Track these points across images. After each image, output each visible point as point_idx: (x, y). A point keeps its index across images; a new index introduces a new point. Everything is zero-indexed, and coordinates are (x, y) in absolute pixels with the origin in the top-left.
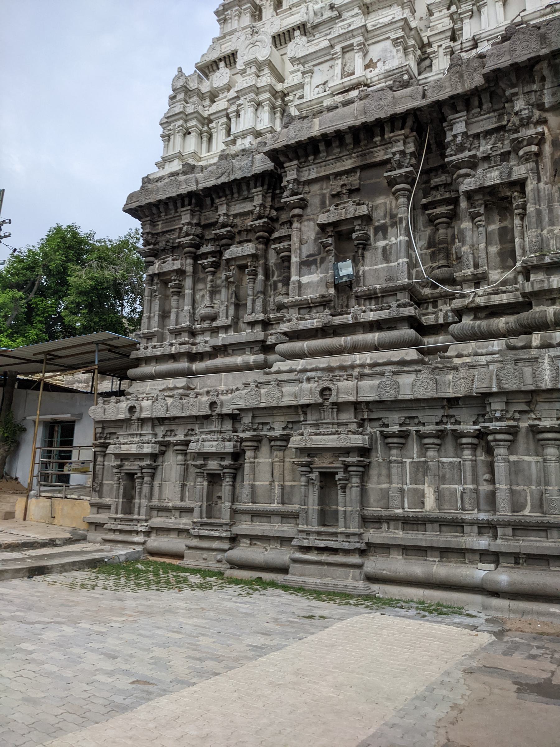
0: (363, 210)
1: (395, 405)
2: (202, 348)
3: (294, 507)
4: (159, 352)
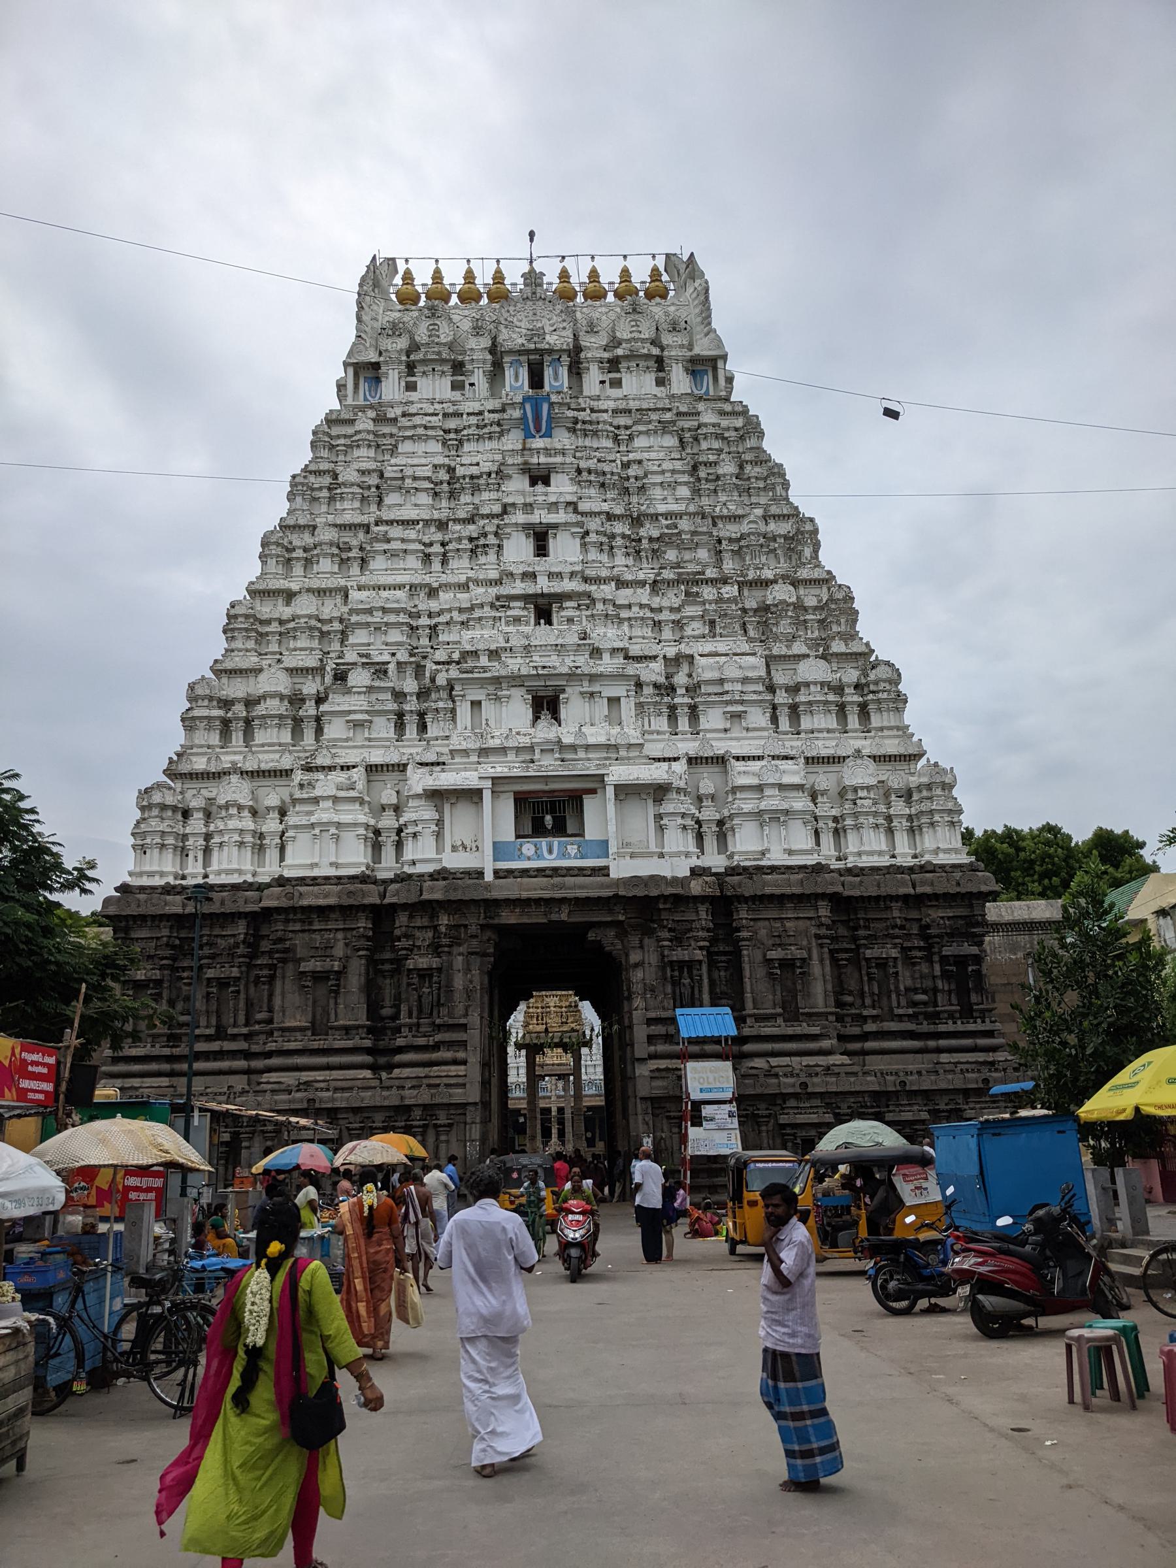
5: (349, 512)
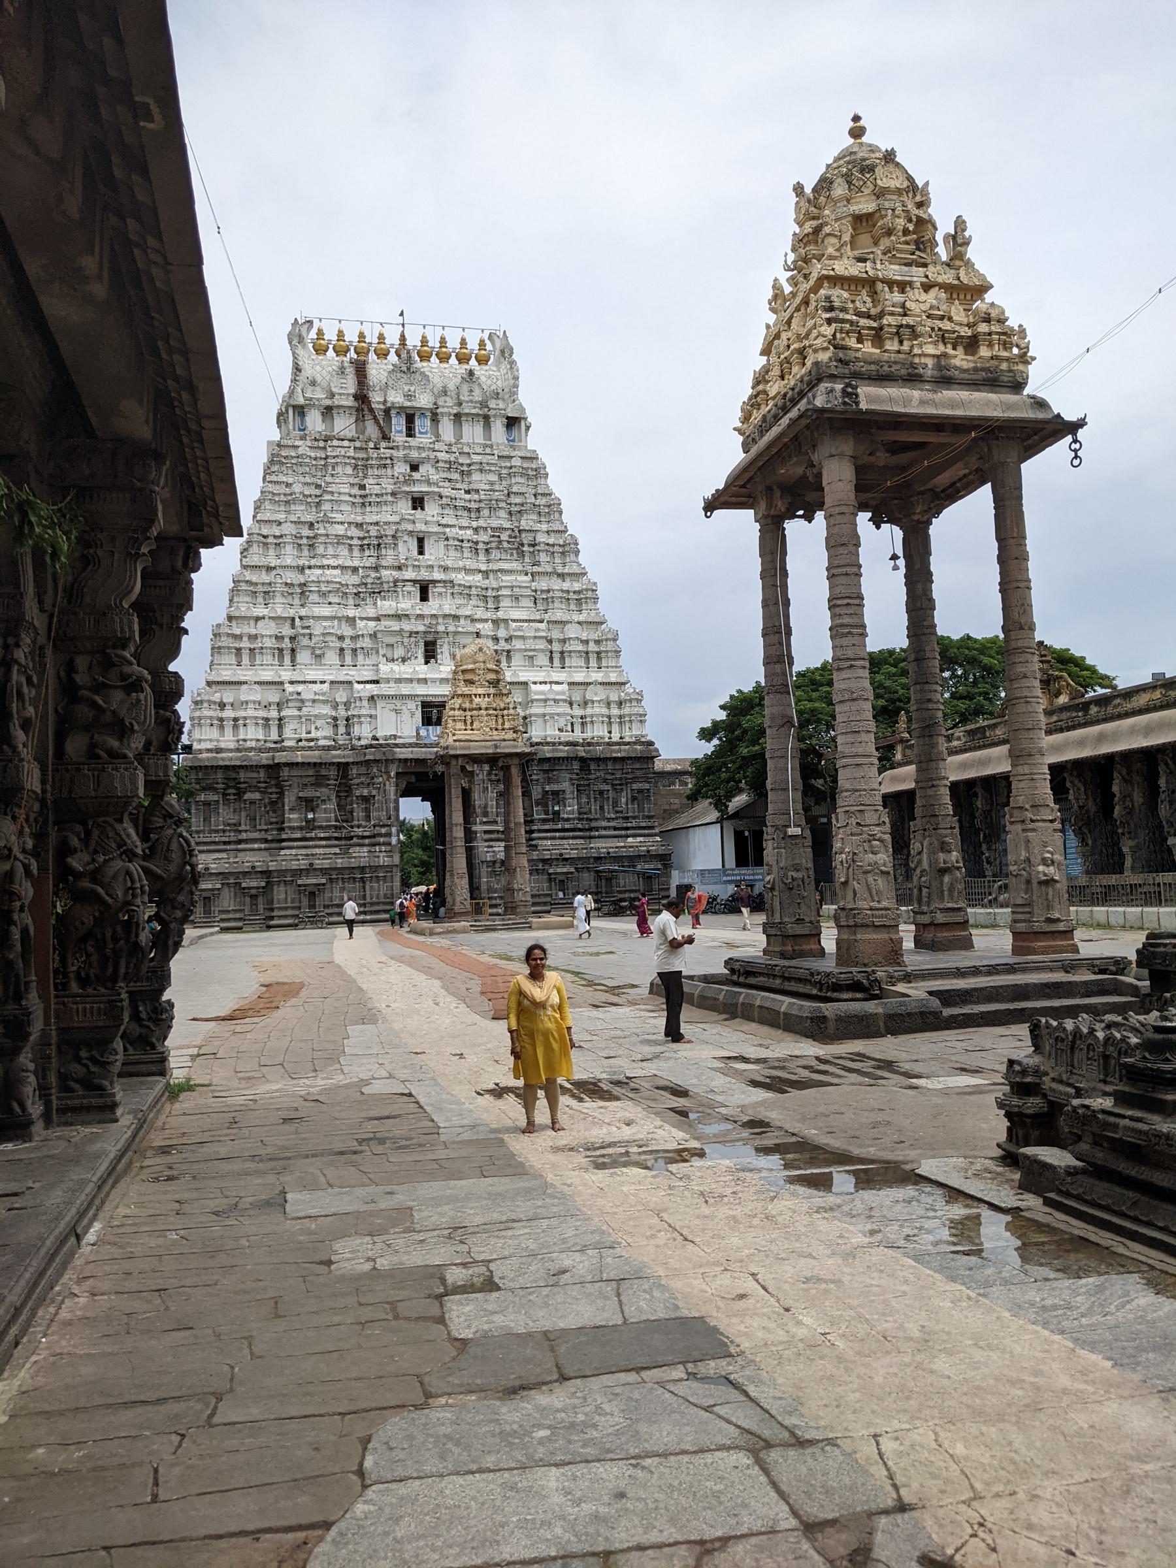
0: (318, 794)
1: (336, 869)
2: (232, 839)
3: (297, 905)
4: (208, 840)
5: (302, 512)
